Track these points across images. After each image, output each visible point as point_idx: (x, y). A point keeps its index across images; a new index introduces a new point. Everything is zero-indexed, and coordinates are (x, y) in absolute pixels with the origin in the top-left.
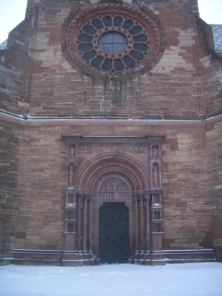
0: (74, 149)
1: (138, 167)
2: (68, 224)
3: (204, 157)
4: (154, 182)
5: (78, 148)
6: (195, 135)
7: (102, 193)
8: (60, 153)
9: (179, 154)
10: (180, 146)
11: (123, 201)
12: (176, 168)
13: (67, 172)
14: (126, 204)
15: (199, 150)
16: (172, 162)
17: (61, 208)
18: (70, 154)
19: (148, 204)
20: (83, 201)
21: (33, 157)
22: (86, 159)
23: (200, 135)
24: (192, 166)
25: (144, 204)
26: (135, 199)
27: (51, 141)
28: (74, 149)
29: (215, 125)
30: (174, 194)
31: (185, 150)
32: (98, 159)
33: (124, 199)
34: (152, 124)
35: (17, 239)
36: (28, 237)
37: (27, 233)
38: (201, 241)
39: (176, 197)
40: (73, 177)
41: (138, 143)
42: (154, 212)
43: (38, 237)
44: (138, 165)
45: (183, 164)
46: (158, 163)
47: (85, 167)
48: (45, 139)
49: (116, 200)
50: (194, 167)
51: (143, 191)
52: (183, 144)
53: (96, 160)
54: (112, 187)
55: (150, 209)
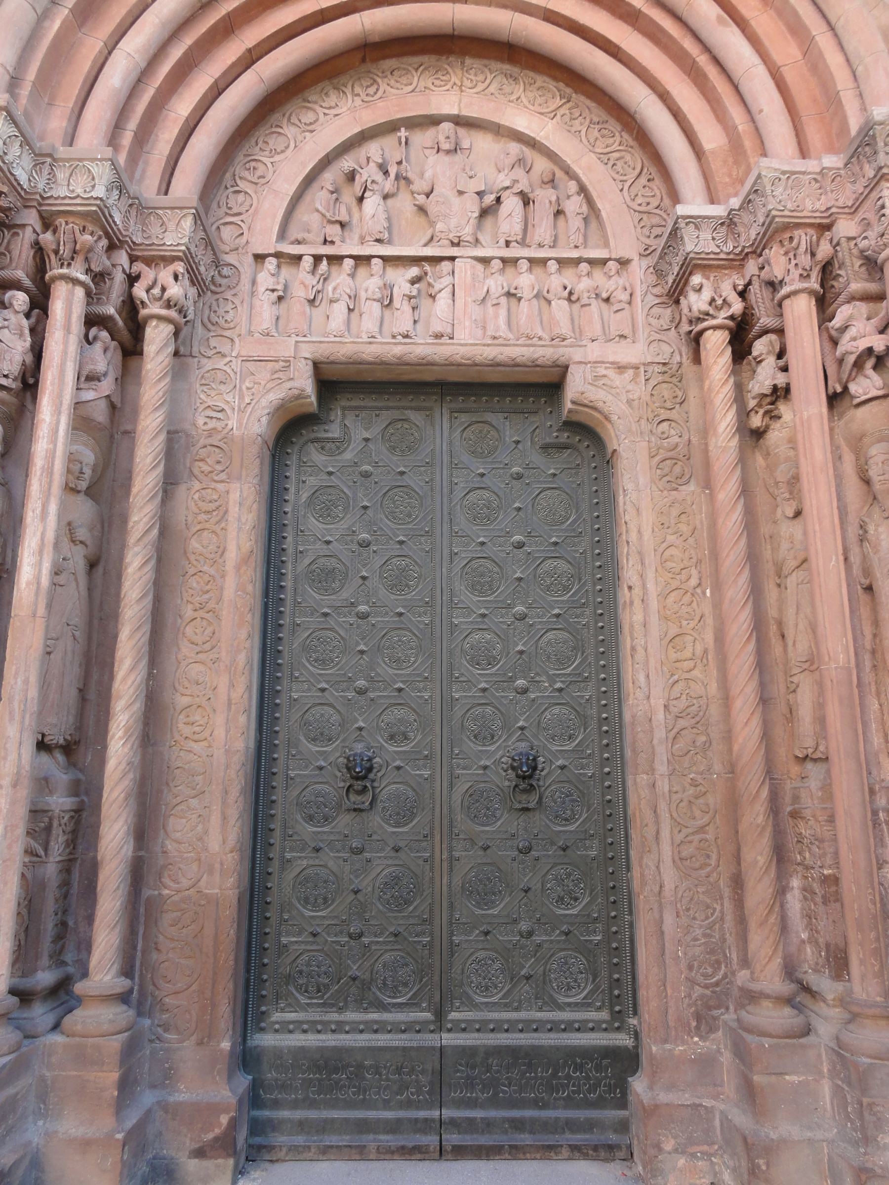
7: (307, 261)
11: (544, 353)
33: (565, 328)
49: (462, 335)
54: (422, 210)
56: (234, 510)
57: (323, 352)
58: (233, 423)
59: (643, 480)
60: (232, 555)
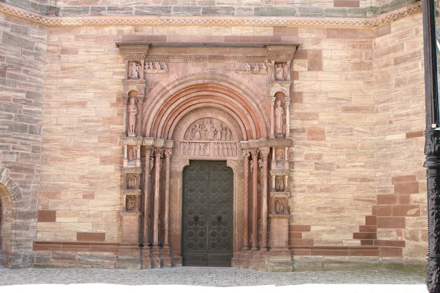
0: (139, 68)
1: (249, 99)
2: (127, 196)
3: (368, 83)
4: (275, 127)
5: (145, 65)
6: (355, 44)
7: (188, 143)
8: (114, 74)
9: (324, 78)
10: (325, 63)
12: (317, 101)
13: (125, 108)
14: (229, 164)
15: (360, 70)
16: (311, 91)
17: (116, 170)
18: (132, 76)
19: (264, 164)
20: (153, 157)
21: (67, 81)
22: (158, 85)
23: (365, 43)
24: (347, 100)
25: (258, 164)
26: (244, 154)
27: (97, 54)
28: (137, 67)
29: (393, 24)
30: (310, 148)
31: (336, 70)
32: (180, 84)
34: (277, 23)
35: (40, 224)
36: (58, 219)
37: (57, 212)
38: (357, 231)
39: (316, 152)
40: (136, 115)
41: (250, 57)
42: (275, 178)
43: (76, 219)
44: (249, 96)
45: (330, 96)
46: (284, 92)
47: (158, 98)
48: (88, 50)
50: (349, 100)
51: (258, 141)
52: (331, 59)
53: (175, 86)
55: (269, 174)
56: (178, 183)
57: (191, 159)
58: (178, 169)
59: (237, 178)
60: (179, 189)
